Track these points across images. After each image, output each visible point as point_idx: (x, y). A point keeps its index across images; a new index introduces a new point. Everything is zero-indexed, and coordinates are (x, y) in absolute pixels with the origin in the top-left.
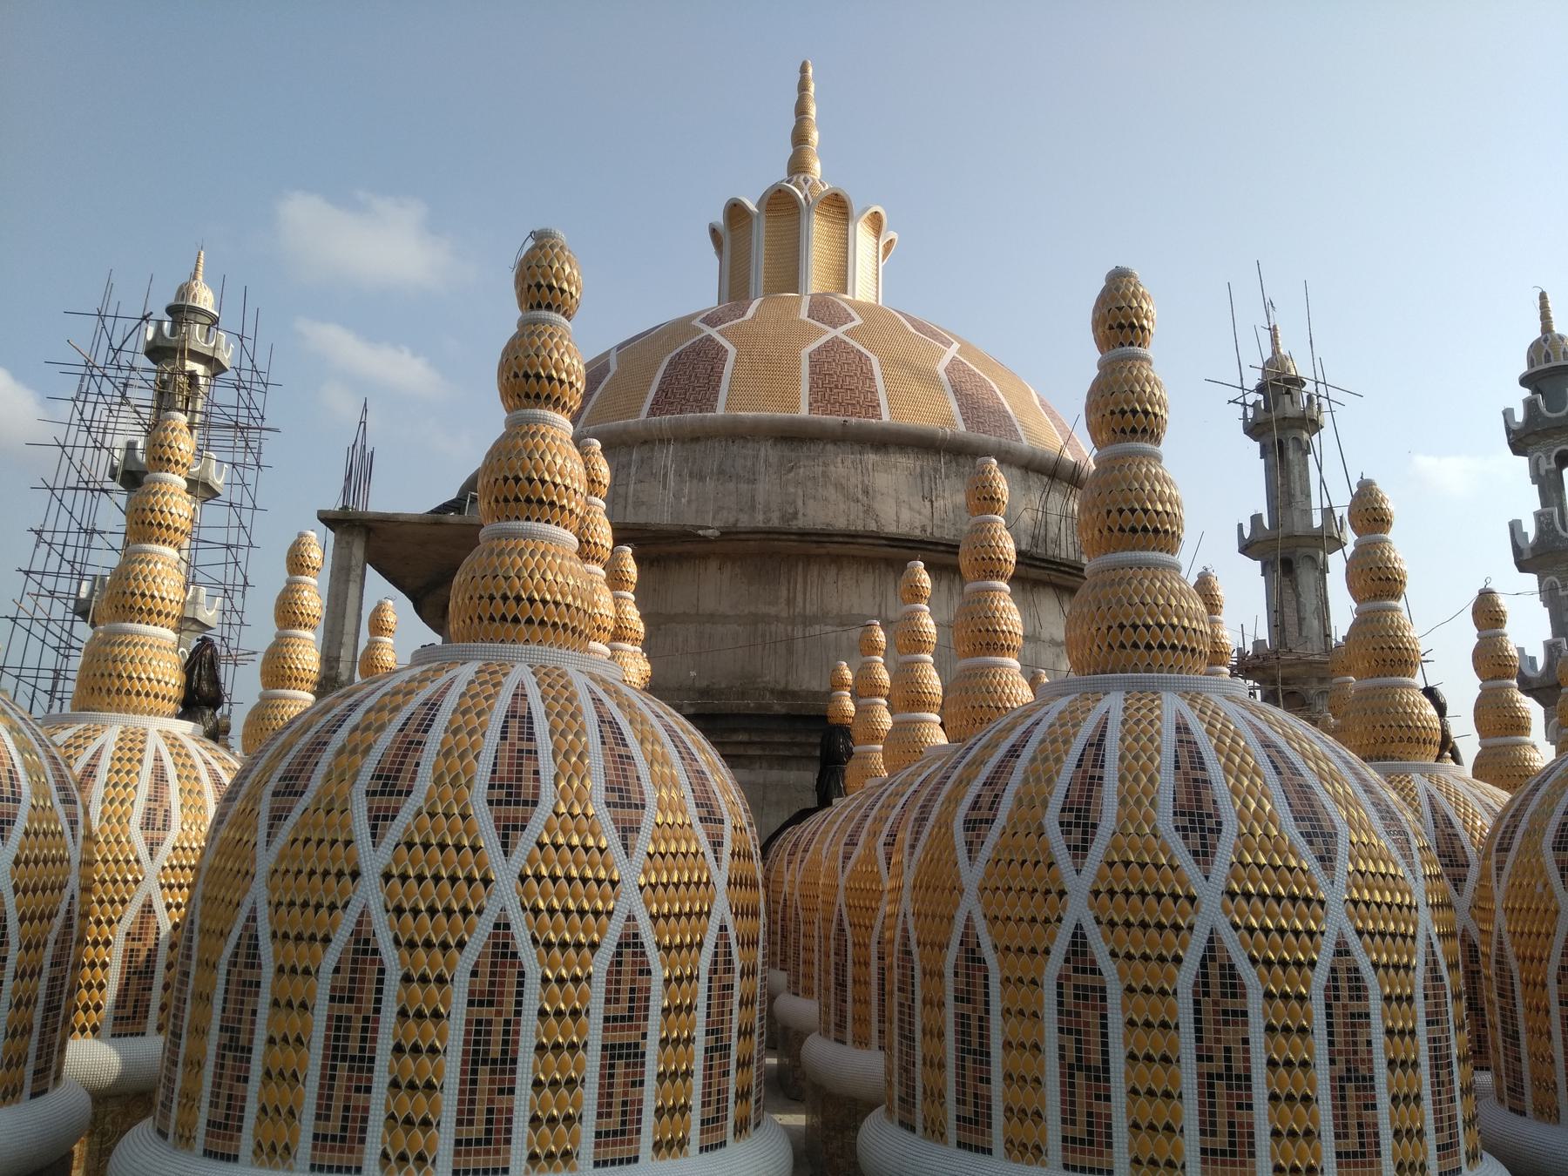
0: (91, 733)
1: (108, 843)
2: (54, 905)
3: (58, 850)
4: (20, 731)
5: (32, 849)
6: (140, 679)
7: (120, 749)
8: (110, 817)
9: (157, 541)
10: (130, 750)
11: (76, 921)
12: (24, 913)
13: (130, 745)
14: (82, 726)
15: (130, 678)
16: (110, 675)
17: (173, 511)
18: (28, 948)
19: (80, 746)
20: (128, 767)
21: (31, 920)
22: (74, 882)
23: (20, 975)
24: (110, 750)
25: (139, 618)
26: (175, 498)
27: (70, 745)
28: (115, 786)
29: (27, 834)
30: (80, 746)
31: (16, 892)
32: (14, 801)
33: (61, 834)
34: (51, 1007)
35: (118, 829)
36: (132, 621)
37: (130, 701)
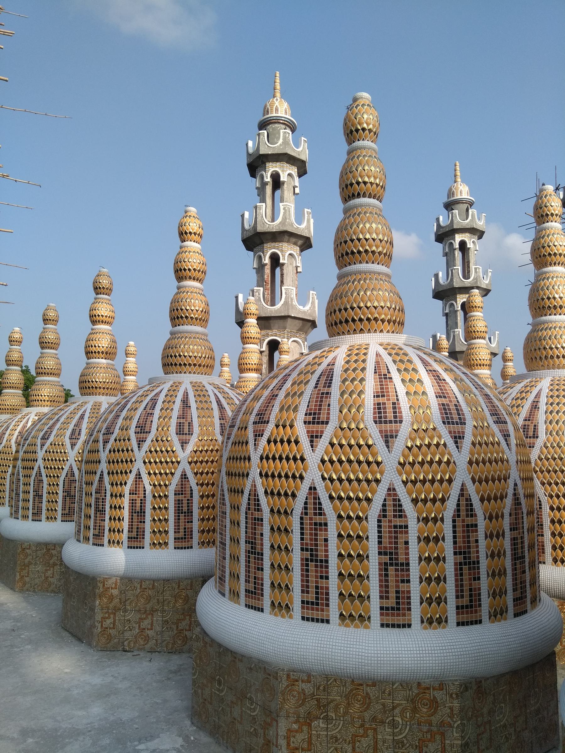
0: (533, 383)
1: (553, 447)
2: (503, 490)
3: (498, 454)
4: (462, 380)
5: (479, 454)
6: (557, 348)
7: (551, 390)
8: (551, 431)
9: (551, 265)
10: (557, 390)
11: (523, 501)
12: (482, 496)
13: (557, 387)
14: (528, 380)
15: (551, 348)
16: (539, 349)
17: (556, 244)
18: (491, 518)
19: (528, 391)
20: (557, 400)
21: (489, 500)
22: (514, 475)
23: (489, 536)
24: (545, 391)
25: (549, 312)
26: (555, 236)
27: (523, 392)
28: (551, 412)
29: (473, 444)
30: (528, 391)
31: (474, 482)
32: (461, 423)
33: (498, 444)
34: (517, 557)
35: (558, 439)
36: (546, 315)
37: (554, 362)
